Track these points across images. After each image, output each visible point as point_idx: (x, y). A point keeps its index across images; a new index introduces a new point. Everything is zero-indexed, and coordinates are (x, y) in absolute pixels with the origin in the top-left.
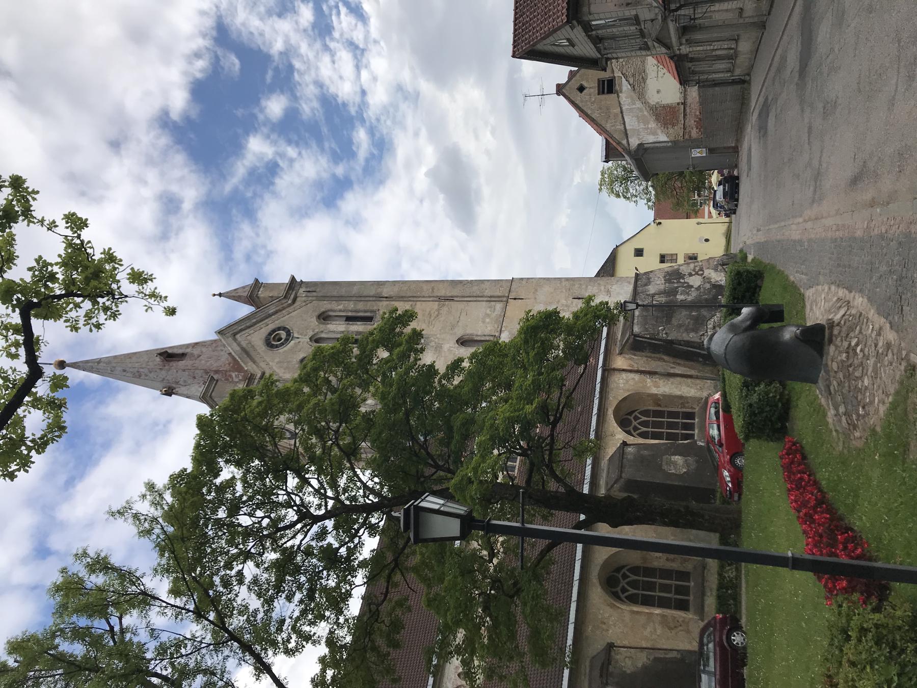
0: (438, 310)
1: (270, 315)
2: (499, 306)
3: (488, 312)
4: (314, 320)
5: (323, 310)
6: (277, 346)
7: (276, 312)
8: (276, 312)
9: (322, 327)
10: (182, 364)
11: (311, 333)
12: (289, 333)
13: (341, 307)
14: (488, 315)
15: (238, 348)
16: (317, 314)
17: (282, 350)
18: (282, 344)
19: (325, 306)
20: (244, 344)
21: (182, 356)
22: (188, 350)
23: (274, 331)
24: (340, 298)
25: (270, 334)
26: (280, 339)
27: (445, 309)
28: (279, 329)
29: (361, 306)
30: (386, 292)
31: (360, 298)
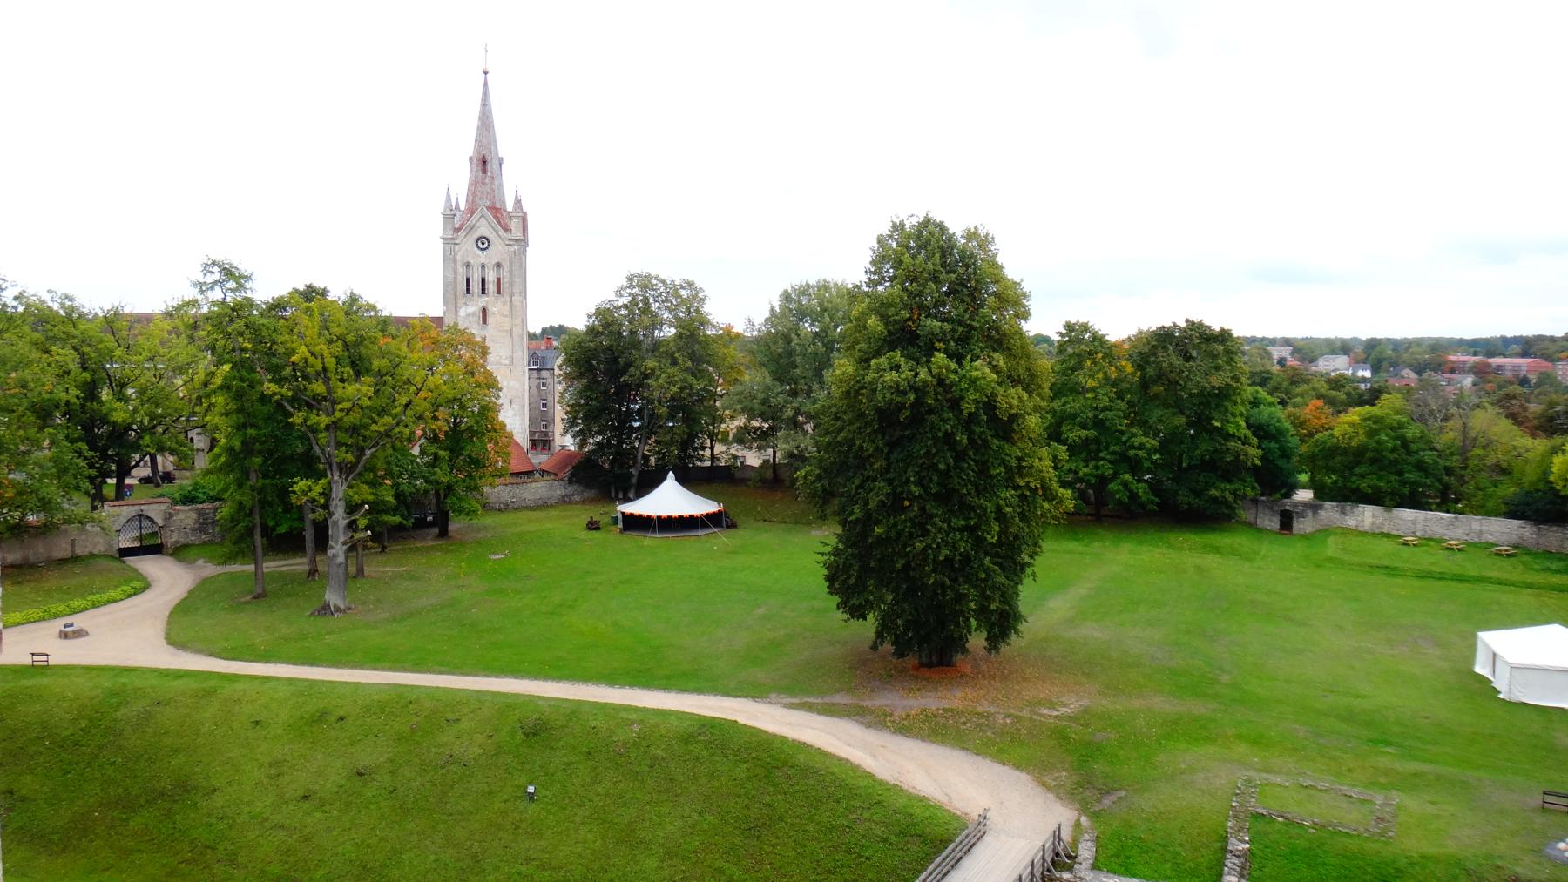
0: (504, 331)
1: (497, 233)
2: (507, 362)
3: (504, 357)
4: (496, 261)
5: (503, 264)
6: (477, 245)
7: (499, 236)
8: (499, 236)
9: (491, 268)
10: (480, 173)
11: (486, 262)
12: (485, 249)
13: (505, 274)
14: (501, 357)
15: (474, 222)
16: (500, 261)
17: (476, 248)
18: (479, 247)
19: (506, 265)
20: (478, 224)
21: (484, 171)
22: (489, 174)
23: (487, 239)
24: (511, 272)
25: (485, 238)
26: (483, 244)
27: (504, 334)
28: (489, 242)
29: (507, 285)
30: (516, 298)
31: (511, 284)
